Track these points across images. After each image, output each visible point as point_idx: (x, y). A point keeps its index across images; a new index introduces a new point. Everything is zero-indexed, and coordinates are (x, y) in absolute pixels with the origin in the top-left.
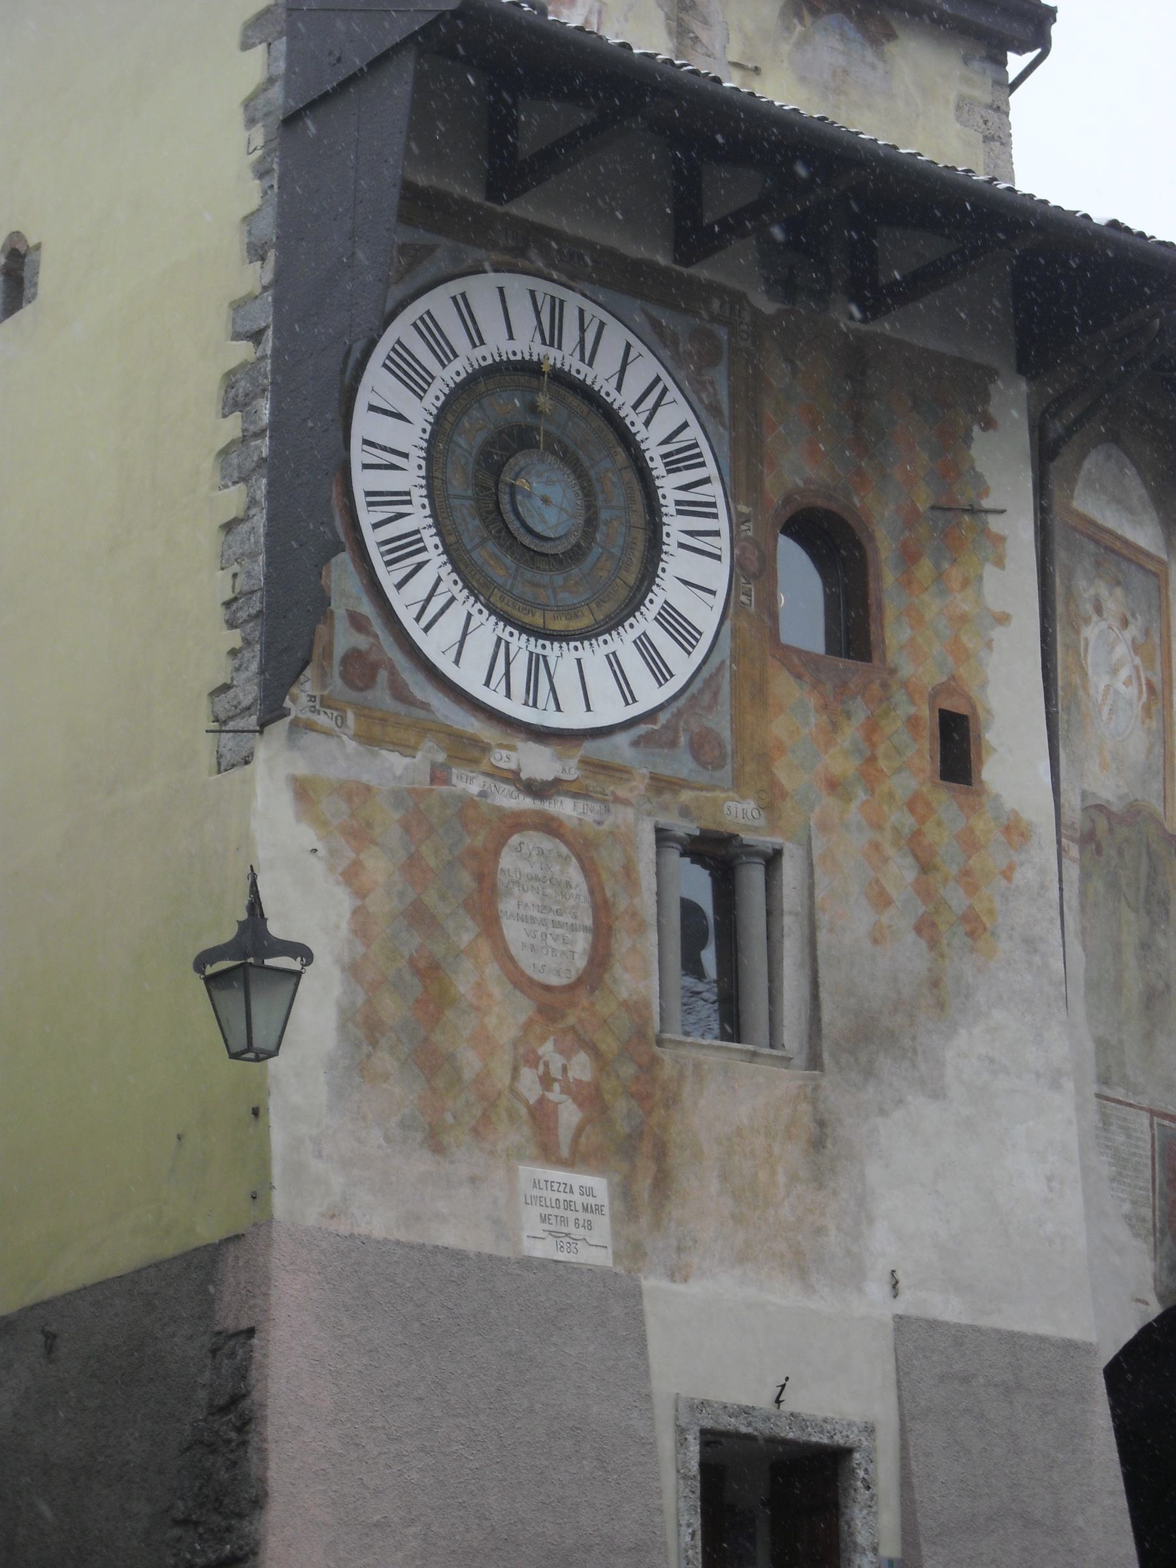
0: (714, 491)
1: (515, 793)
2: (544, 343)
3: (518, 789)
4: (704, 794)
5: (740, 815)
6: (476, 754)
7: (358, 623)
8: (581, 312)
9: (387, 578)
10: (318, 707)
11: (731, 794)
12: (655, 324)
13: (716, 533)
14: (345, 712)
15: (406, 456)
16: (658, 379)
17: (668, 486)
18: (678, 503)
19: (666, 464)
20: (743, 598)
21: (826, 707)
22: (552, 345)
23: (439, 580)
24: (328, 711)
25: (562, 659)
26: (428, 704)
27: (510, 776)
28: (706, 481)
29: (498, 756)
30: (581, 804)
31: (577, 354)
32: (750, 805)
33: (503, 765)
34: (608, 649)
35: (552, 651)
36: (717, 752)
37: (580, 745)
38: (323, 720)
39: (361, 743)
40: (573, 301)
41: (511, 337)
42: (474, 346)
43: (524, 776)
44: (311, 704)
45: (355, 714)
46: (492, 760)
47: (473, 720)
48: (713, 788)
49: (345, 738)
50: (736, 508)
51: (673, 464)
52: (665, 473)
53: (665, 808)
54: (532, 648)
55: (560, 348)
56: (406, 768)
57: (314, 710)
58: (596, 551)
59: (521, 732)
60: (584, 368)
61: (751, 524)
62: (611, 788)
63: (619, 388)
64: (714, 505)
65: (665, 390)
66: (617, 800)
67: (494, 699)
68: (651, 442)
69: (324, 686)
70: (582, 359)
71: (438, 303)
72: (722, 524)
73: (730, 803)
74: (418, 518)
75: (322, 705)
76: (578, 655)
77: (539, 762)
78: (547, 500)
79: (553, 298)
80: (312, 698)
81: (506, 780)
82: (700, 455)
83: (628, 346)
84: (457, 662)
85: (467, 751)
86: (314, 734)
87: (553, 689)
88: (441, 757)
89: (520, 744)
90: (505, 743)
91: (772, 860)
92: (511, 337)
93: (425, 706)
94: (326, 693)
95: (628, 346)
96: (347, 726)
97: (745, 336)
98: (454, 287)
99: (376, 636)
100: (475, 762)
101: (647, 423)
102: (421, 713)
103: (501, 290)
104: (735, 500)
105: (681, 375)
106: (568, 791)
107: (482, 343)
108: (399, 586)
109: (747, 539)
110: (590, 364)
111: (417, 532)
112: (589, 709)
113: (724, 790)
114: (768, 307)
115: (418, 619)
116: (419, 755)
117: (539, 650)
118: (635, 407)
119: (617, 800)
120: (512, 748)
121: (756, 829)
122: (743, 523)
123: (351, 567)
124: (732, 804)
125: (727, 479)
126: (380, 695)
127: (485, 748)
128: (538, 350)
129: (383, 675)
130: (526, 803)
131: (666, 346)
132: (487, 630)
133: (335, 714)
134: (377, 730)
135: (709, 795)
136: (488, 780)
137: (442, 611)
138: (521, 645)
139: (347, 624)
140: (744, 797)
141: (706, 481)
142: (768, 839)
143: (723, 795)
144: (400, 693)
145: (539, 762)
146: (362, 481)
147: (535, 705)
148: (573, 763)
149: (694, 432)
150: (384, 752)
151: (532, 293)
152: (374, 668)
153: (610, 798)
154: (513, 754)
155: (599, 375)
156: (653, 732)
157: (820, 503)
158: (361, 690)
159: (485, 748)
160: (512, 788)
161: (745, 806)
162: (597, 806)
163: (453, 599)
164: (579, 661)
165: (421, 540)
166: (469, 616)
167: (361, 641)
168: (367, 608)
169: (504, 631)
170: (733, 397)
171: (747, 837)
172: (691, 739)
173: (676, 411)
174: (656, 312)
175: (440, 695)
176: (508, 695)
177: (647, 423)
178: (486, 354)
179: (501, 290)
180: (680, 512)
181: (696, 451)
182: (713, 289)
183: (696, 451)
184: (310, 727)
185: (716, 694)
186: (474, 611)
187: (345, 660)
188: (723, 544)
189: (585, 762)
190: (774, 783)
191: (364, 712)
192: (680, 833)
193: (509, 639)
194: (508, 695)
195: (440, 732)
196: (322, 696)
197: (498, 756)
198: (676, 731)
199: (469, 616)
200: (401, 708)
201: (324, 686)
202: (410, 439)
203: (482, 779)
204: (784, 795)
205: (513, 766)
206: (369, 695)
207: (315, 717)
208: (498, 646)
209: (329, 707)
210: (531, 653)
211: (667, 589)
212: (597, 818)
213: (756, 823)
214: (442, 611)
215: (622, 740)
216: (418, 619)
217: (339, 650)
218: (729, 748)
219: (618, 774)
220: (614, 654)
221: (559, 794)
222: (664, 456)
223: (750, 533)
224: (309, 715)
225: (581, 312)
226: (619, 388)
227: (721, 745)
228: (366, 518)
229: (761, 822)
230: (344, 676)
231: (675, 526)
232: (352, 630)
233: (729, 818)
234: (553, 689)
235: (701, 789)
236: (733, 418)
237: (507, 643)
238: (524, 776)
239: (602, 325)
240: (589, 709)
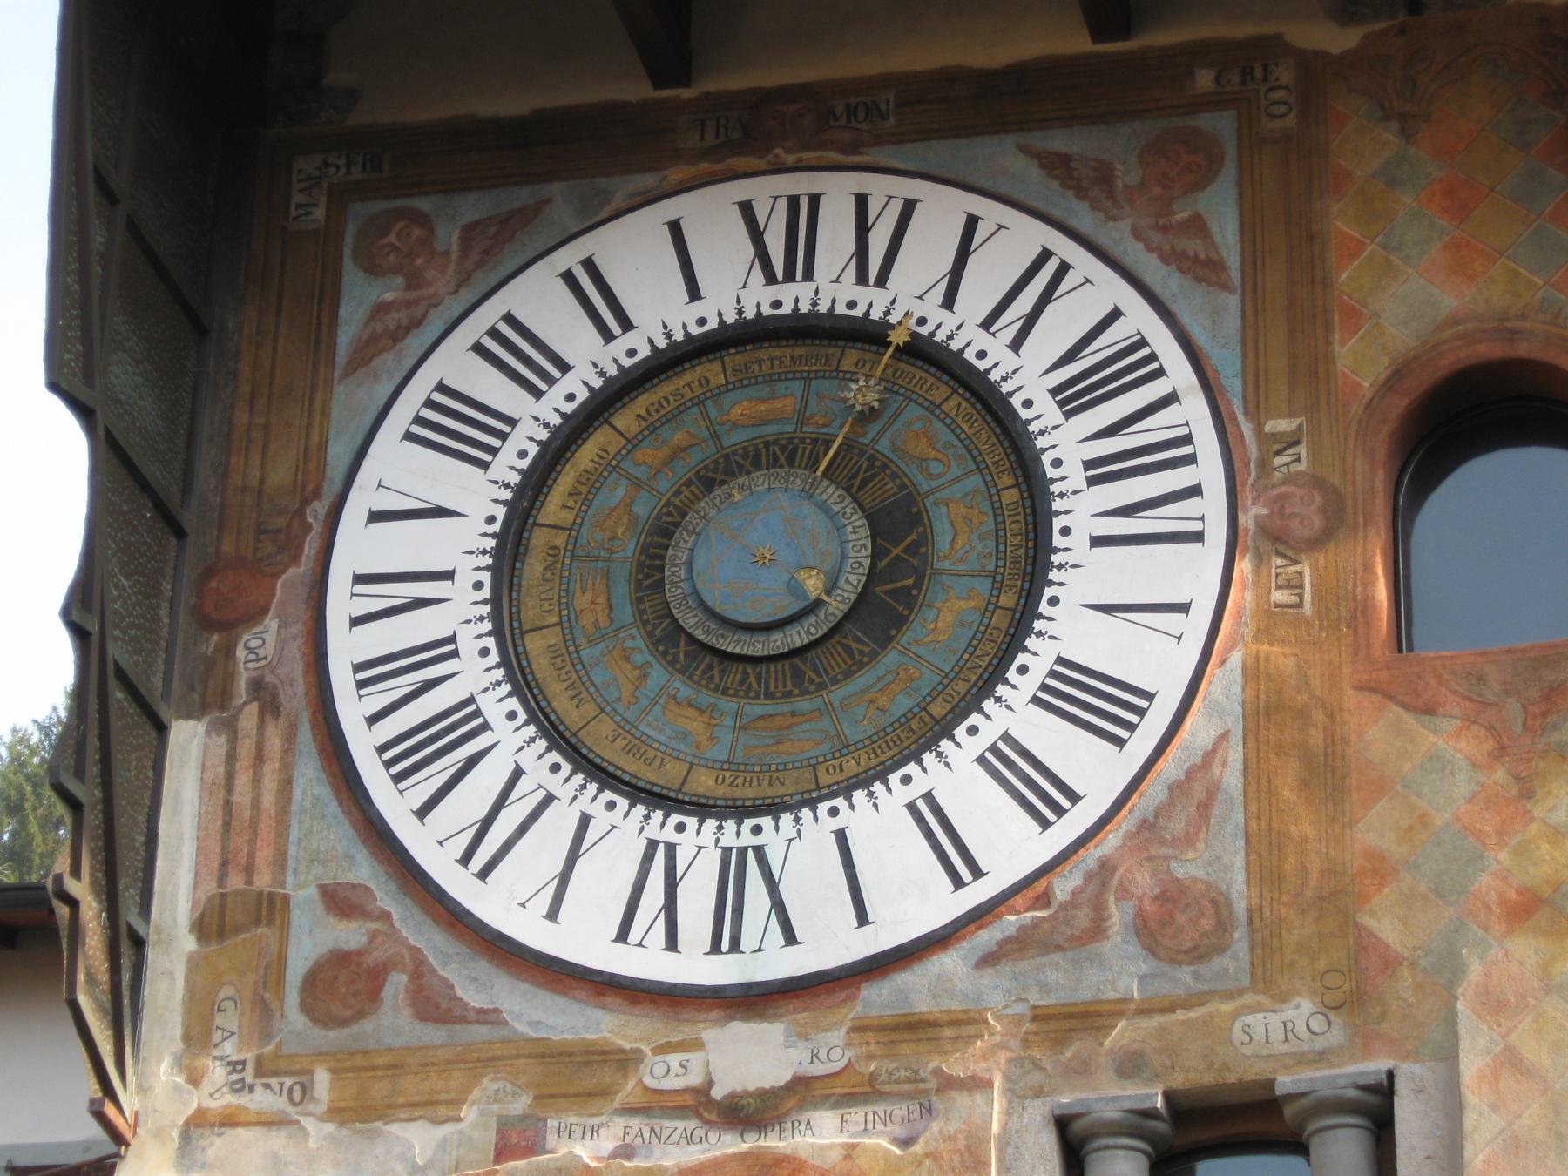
0: (1194, 413)
1: (700, 1132)
2: (771, 279)
3: (708, 1122)
4: (1180, 1015)
5: (1277, 1035)
6: (606, 1076)
7: (340, 902)
8: (861, 202)
9: (394, 805)
10: (249, 1080)
11: (1249, 999)
12: (1058, 166)
13: (1195, 491)
14: (311, 1073)
15: (448, 575)
16: (1046, 255)
17: (1066, 444)
18: (1089, 465)
19: (1061, 404)
20: (1279, 596)
21: (1502, 750)
22: (790, 277)
23: (518, 773)
24: (274, 1081)
25: (800, 847)
26: (497, 1011)
27: (689, 1100)
28: (1170, 399)
29: (659, 1070)
30: (856, 1115)
31: (758, 275)
32: (1302, 1010)
33: (673, 1083)
34: (914, 791)
35: (774, 834)
36: (1207, 923)
37: (854, 997)
38: (262, 1100)
39: (342, 1123)
40: (837, 192)
41: (694, 294)
42: (608, 337)
43: (717, 1093)
44: (235, 1077)
45: (333, 1071)
46: (649, 1081)
47: (598, 1015)
48: (1201, 999)
49: (309, 1123)
50: (1259, 431)
51: (1073, 398)
52: (1060, 419)
53: (1082, 1070)
54: (729, 839)
55: (808, 276)
56: (443, 1145)
57: (239, 1087)
58: (626, 613)
59: (709, 1009)
60: (864, 295)
61: (1302, 450)
62: (931, 1066)
63: (949, 302)
64: (1187, 440)
65: (1064, 268)
66: (948, 1084)
67: (646, 961)
68: (1028, 377)
69: (265, 1036)
70: (862, 279)
71: (539, 298)
72: (1210, 469)
73: (1248, 1019)
74: (475, 674)
75: (261, 1071)
76: (836, 824)
77: (750, 1057)
78: (777, 552)
79: (794, 202)
80: (236, 1066)
81: (680, 1111)
82: (1152, 357)
83: (972, 222)
84: (553, 914)
85: (579, 1078)
86: (240, 1131)
87: (778, 906)
88: (520, 1105)
89: (710, 1034)
90: (675, 1039)
91: (1376, 1111)
92: (694, 294)
93: (489, 1016)
94: (269, 1049)
95: (972, 222)
96: (313, 1099)
97: (1282, 109)
98: (569, 257)
99: (386, 916)
100: (605, 1093)
101: (1016, 345)
102: (481, 1032)
103: (675, 228)
104: (1256, 412)
105: (1117, 235)
106: (828, 1096)
107: (627, 325)
108: (423, 812)
109: (1289, 480)
110: (881, 281)
111: (471, 700)
112: (863, 919)
113: (1229, 995)
114: (1338, 40)
115: (465, 859)
116: (469, 1113)
117: (747, 839)
118: (987, 324)
119: (948, 1084)
120: (696, 1045)
121: (1321, 1057)
122: (1278, 453)
123: (333, 807)
124: (1256, 1020)
125: (1233, 386)
126: (393, 1022)
127: (626, 1061)
128: (759, 298)
129: (397, 984)
130: (731, 1144)
131: (1081, 194)
132: (624, 831)
133: (288, 1081)
134: (380, 1089)
135: (1192, 1014)
136: (636, 1123)
137: (523, 829)
138: (701, 845)
139: (320, 908)
140: (1282, 998)
141: (1170, 399)
142: (1350, 1069)
143: (1226, 1008)
144: (434, 1004)
145: (750, 1057)
146: (346, 649)
147: (735, 946)
148: (837, 1036)
149: (1140, 319)
150: (395, 1128)
151: (746, 209)
152: (377, 976)
153: (932, 1084)
154: (695, 1059)
155: (908, 297)
156: (1036, 923)
157: (1490, 350)
158: (344, 1023)
159: (626, 1061)
160: (692, 1124)
161: (1289, 1014)
162: (900, 1110)
163: (549, 799)
164: (841, 836)
165: (477, 713)
166: (585, 820)
167: (350, 935)
168: (364, 871)
169: (662, 827)
170: (1250, 230)
171: (1285, 1083)
172: (1140, 915)
173: (1094, 291)
174: (1057, 141)
175: (525, 987)
176: (672, 943)
177: (1016, 345)
178: (638, 344)
179: (675, 228)
180: (1093, 481)
181: (1145, 352)
182: (1199, 53)
183: (1145, 352)
184: (229, 1120)
185: (1204, 807)
186: (597, 810)
187: (311, 980)
188: (1212, 509)
189: (859, 1028)
190: (1364, 946)
191: (346, 1065)
192: (1112, 1113)
193: (757, 841)
194: (672, 943)
195: (518, 1056)
196: (259, 1061)
197: (659, 1070)
198: (1099, 908)
199: (585, 820)
200: (433, 1034)
201: (265, 1036)
202: (463, 545)
203: (620, 1122)
204: (1390, 963)
205: (695, 1079)
206: (367, 1026)
207: (244, 1100)
208: (648, 858)
209: (275, 1074)
210: (727, 851)
211: (1068, 630)
212: (901, 1132)
213: (1320, 1043)
214: (523, 829)
215: (950, 962)
216: (465, 859)
217: (298, 965)
218: (1240, 907)
219: (948, 1032)
220: (929, 797)
221: (803, 1106)
222: (1054, 392)
223: (1303, 466)
224: (230, 1099)
225: (861, 202)
226: (949, 302)
227: (1219, 904)
228: (351, 709)
229: (1336, 1036)
230: (306, 1008)
231: (1080, 510)
232: (331, 919)
233: (1247, 1050)
234: (778, 906)
235: (1171, 1009)
236: (1252, 261)
237: (671, 849)
238: (717, 1093)
239: (909, 207)
240: (863, 919)
